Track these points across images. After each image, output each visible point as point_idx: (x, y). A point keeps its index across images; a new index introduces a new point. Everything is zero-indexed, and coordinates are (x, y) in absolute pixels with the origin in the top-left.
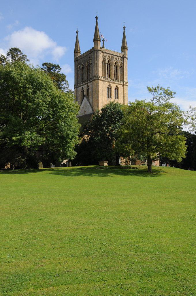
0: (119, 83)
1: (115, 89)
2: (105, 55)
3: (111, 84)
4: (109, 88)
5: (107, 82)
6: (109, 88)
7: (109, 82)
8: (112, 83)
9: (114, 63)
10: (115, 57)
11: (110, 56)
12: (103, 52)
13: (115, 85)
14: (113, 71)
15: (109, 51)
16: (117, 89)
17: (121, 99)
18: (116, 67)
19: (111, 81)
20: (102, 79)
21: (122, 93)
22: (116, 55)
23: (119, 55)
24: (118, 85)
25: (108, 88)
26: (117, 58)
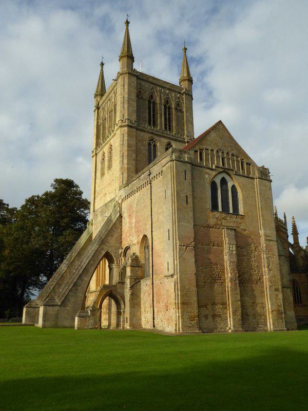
0: (112, 134)
13: (107, 147)
25: (103, 159)
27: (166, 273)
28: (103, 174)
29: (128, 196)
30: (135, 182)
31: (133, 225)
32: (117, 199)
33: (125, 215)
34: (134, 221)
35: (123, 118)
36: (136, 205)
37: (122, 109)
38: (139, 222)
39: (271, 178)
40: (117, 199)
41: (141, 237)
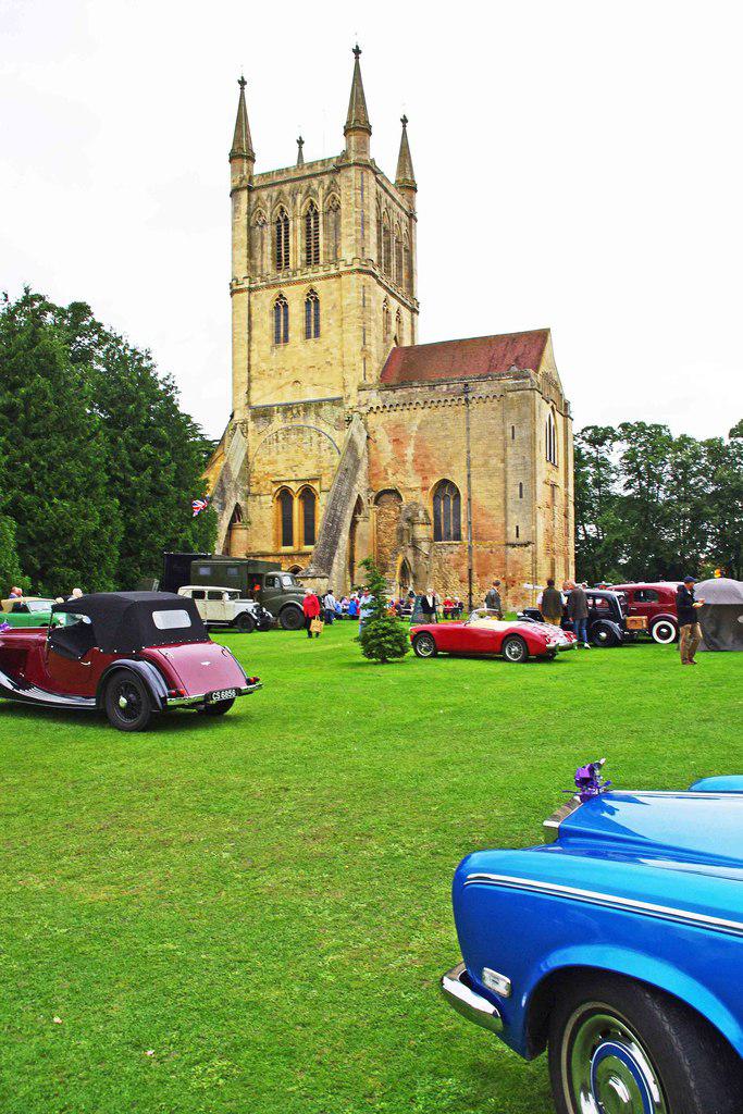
1: (308, 303)
2: (264, 194)
3: (286, 291)
4: (281, 307)
5: (268, 287)
6: (281, 307)
7: (274, 286)
8: (289, 284)
9: (302, 211)
10: (304, 184)
11: (287, 188)
12: (250, 190)
13: (304, 288)
14: (297, 242)
15: (280, 172)
16: (312, 301)
17: (329, 331)
18: (311, 215)
19: (284, 280)
20: (246, 285)
21: (334, 306)
22: (307, 173)
23: (319, 169)
24: (314, 284)
25: (277, 307)
26: (315, 182)
27: (512, 539)
28: (281, 337)
29: (386, 407)
30: (419, 389)
31: (410, 458)
32: (352, 403)
33: (382, 437)
34: (410, 451)
35: (363, 255)
36: (419, 428)
37: (359, 237)
38: (427, 457)
39: (572, 416)
40: (352, 403)
41: (433, 481)
